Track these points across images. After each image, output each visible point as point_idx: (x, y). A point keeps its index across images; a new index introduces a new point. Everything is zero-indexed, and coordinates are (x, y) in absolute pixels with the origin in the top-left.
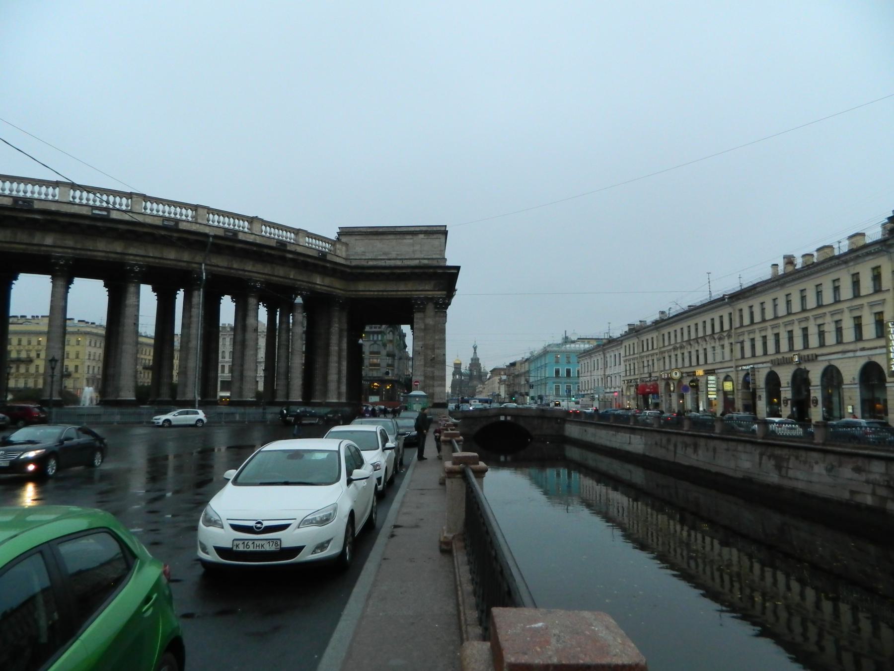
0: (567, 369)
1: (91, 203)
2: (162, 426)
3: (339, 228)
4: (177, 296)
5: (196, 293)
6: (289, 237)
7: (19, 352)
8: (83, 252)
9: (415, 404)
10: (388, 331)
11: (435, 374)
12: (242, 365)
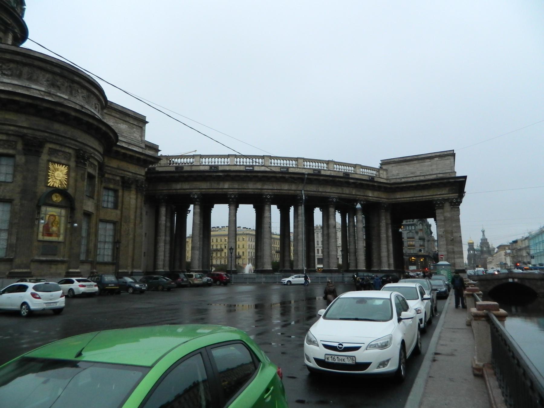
1: (245, 164)
2: (287, 284)
3: (381, 160)
4: (290, 210)
5: (300, 208)
6: (351, 170)
7: (217, 246)
8: (242, 190)
9: (441, 270)
10: (418, 224)
12: (328, 248)
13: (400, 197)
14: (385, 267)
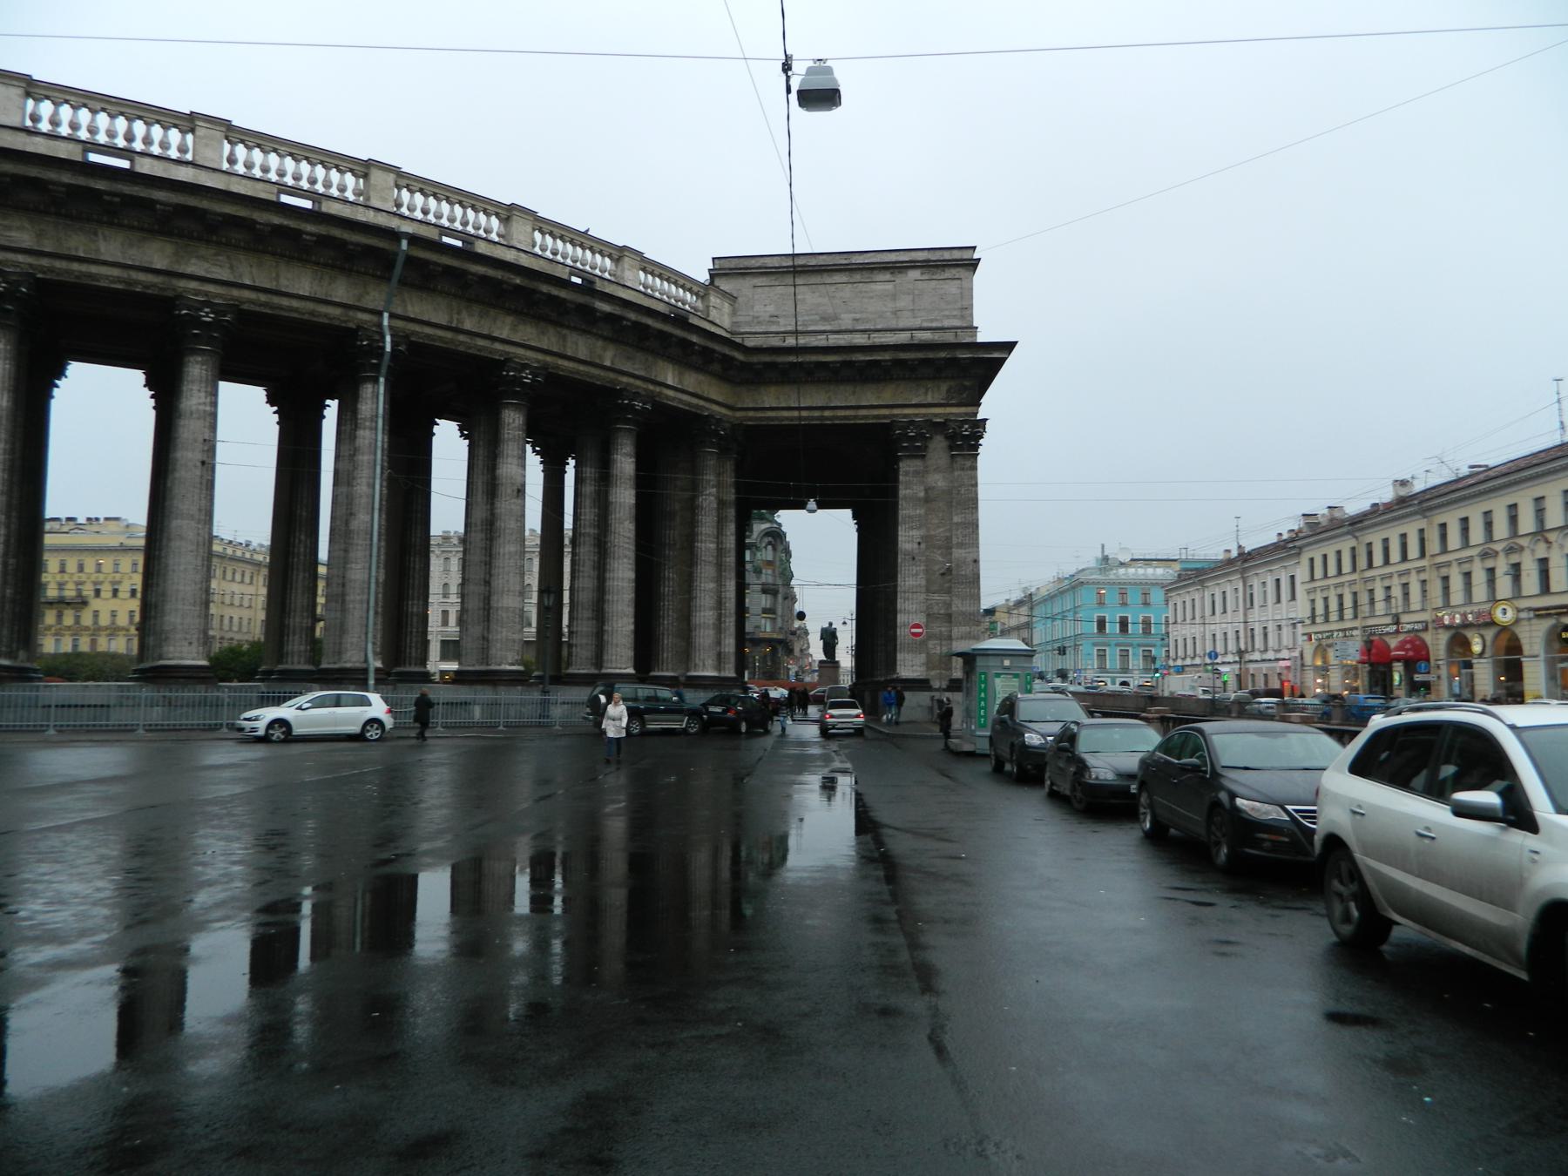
0: (1121, 617)
1: (83, 134)
2: (265, 740)
4: (326, 412)
5: (367, 390)
6: (602, 265)
7: (61, 586)
8: (59, 264)
9: (998, 675)
10: (764, 545)
11: (954, 608)
12: (488, 583)
13: (774, 405)
14: (704, 665)
